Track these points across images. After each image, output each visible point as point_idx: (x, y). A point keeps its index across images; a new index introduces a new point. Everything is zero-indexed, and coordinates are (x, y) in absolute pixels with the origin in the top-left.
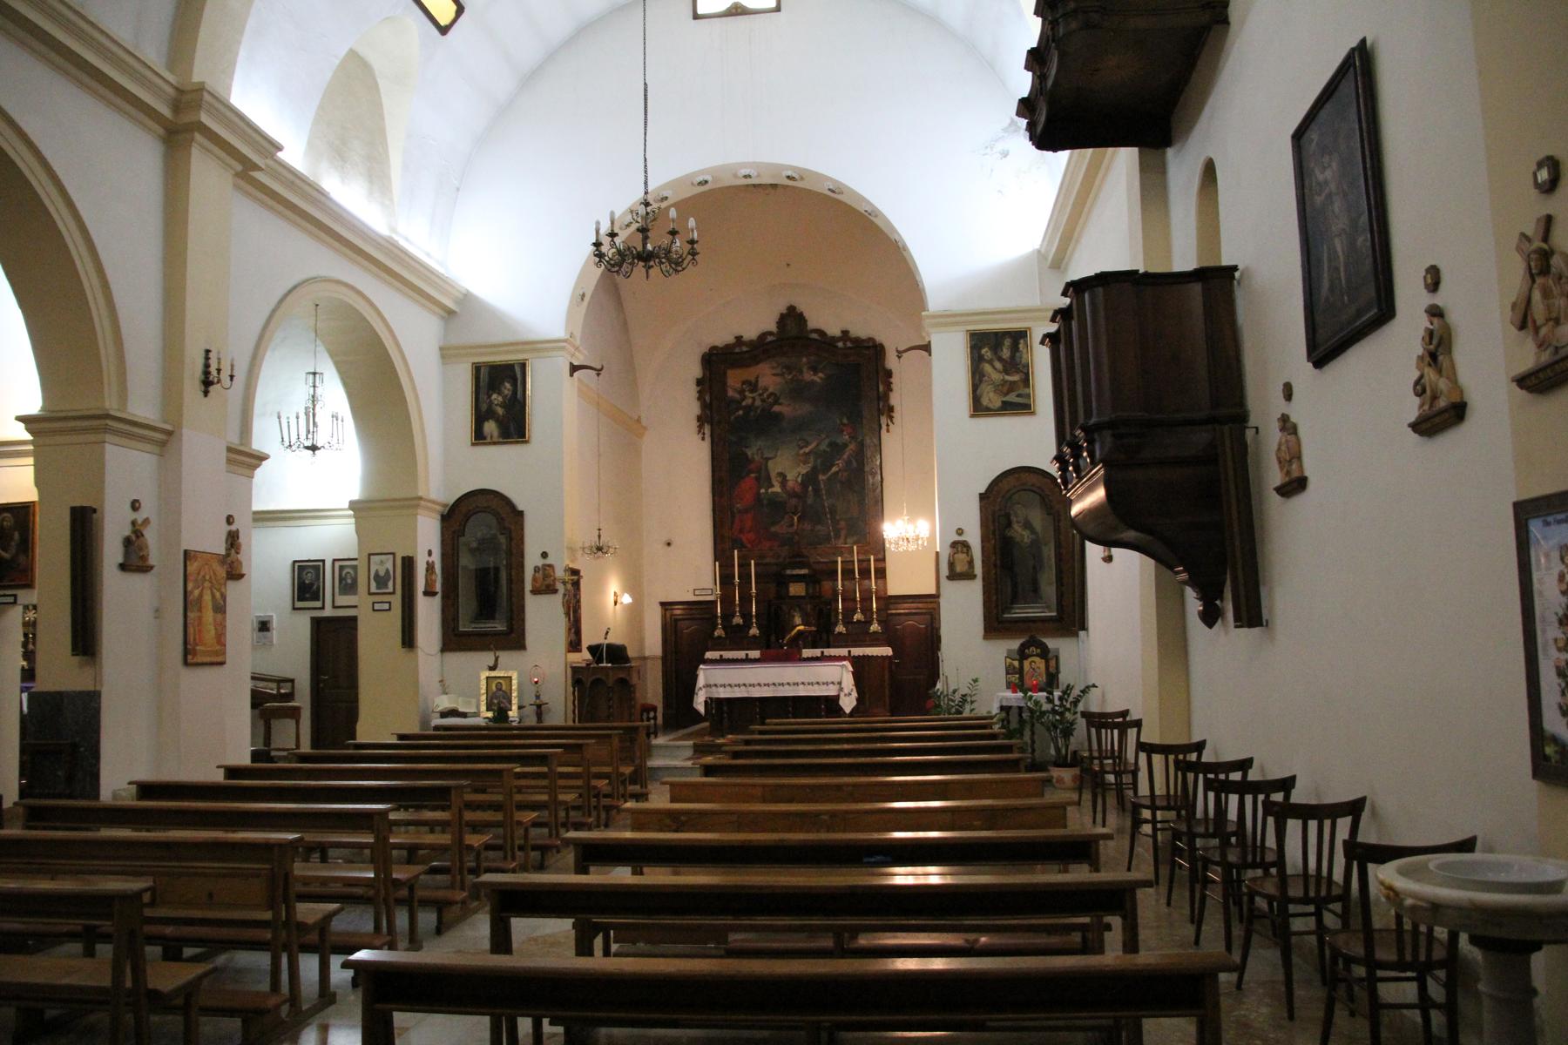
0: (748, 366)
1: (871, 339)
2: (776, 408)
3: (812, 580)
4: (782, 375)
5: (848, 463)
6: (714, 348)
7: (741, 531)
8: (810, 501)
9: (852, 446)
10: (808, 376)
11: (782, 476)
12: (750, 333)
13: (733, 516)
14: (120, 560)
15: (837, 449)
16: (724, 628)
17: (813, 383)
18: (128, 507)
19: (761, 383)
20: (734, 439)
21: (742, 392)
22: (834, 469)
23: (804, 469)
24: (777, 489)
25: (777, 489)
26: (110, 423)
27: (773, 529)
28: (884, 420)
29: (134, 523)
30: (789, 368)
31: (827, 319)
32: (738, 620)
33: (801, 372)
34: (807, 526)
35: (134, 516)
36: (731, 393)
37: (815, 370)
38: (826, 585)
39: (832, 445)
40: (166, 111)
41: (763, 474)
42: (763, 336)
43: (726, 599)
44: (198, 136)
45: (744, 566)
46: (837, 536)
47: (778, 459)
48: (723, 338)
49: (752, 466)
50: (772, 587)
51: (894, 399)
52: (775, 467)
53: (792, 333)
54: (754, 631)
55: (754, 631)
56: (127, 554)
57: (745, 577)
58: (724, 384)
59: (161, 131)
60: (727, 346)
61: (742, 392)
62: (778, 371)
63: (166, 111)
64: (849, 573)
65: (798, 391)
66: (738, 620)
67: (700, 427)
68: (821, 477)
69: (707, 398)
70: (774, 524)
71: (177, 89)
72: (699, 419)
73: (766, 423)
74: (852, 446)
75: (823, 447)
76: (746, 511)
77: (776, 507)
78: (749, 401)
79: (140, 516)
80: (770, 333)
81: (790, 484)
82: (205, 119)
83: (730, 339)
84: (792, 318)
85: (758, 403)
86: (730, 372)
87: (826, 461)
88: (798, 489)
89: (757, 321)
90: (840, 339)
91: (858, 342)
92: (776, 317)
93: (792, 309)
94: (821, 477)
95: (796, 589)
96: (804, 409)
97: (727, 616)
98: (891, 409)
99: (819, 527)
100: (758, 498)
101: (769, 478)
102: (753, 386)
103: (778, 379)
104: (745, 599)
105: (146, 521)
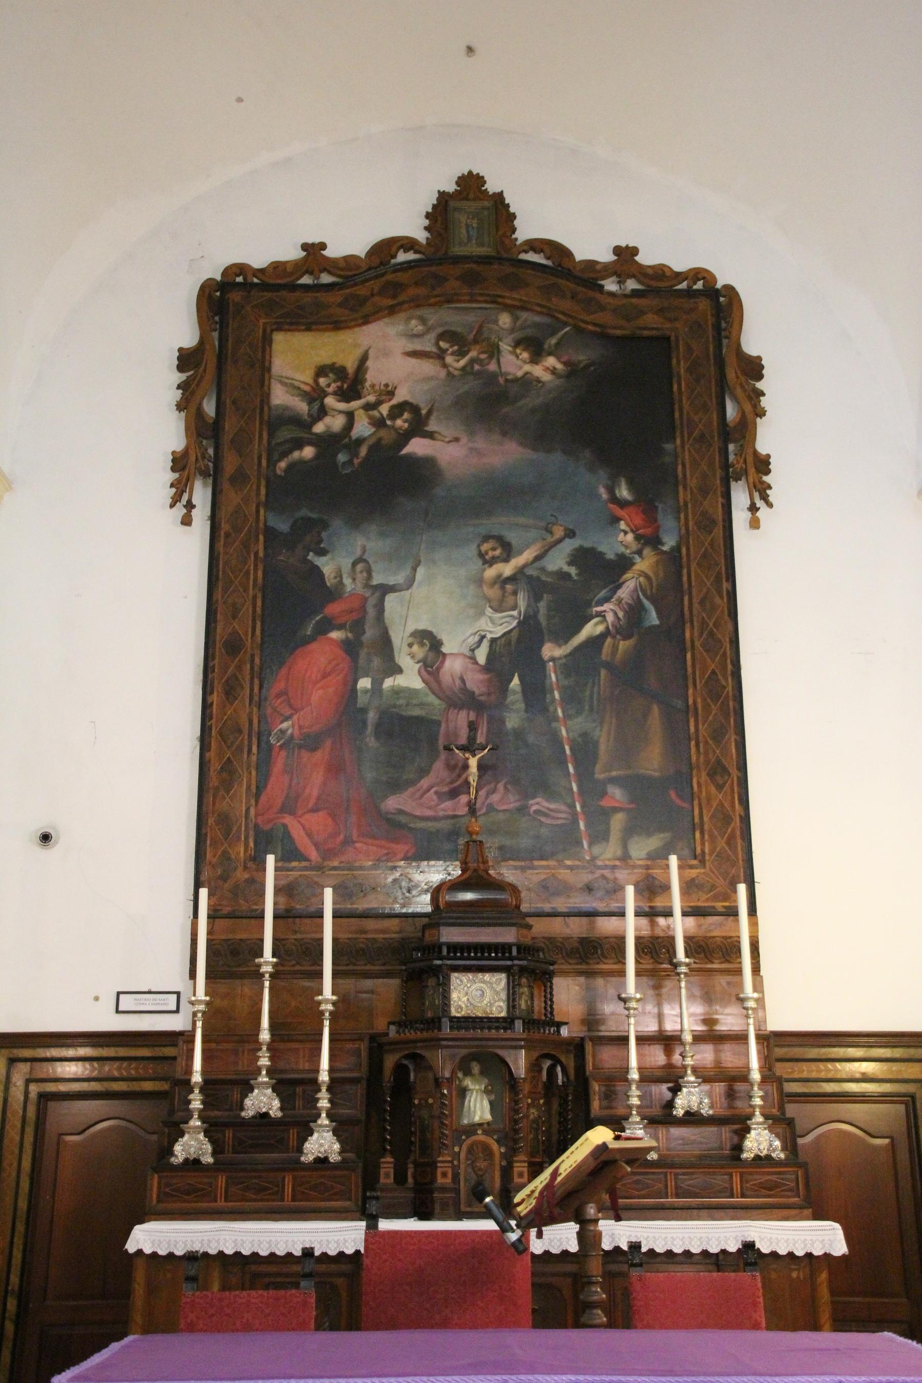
0: (337, 325)
1: (698, 274)
2: (417, 447)
3: (530, 966)
4: (440, 356)
5: (635, 611)
6: (241, 269)
7: (289, 807)
8: (512, 721)
9: (644, 564)
10: (514, 363)
11: (430, 642)
12: (349, 241)
13: (267, 752)
15: (603, 571)
16: (212, 1130)
17: (527, 382)
19: (376, 375)
20: (283, 525)
21: (315, 396)
22: (591, 629)
23: (499, 625)
24: (410, 679)
25: (410, 679)
27: (392, 803)
28: (740, 497)
30: (458, 340)
31: (570, 212)
32: (263, 1100)
33: (494, 352)
34: (502, 798)
36: (280, 397)
37: (537, 353)
38: (568, 995)
39: (586, 558)
41: (370, 633)
42: (385, 249)
43: (227, 1029)
45: (296, 916)
46: (600, 836)
47: (418, 591)
48: (268, 245)
49: (333, 609)
50: (385, 991)
51: (767, 440)
52: (404, 616)
53: (469, 250)
54: (322, 1143)
55: (322, 1143)
57: (299, 956)
58: (266, 369)
60: (277, 267)
61: (315, 396)
62: (427, 345)
64: (655, 950)
65: (488, 404)
66: (263, 1100)
67: (181, 489)
68: (550, 651)
69: (210, 408)
70: (395, 786)
72: (179, 462)
73: (382, 483)
74: (644, 564)
75: (558, 561)
76: (311, 742)
77: (408, 735)
78: (336, 423)
80: (408, 244)
81: (453, 667)
83: (291, 253)
84: (471, 208)
85: (362, 428)
86: (279, 339)
87: (560, 602)
88: (476, 682)
89: (370, 209)
90: (607, 270)
91: (659, 281)
92: (428, 201)
93: (471, 184)
94: (550, 651)
95: (476, 994)
96: (503, 454)
97: (225, 1088)
98: (763, 464)
99: (538, 803)
100: (349, 707)
101: (385, 644)
102: (351, 384)
103: (428, 368)
104: (295, 1030)
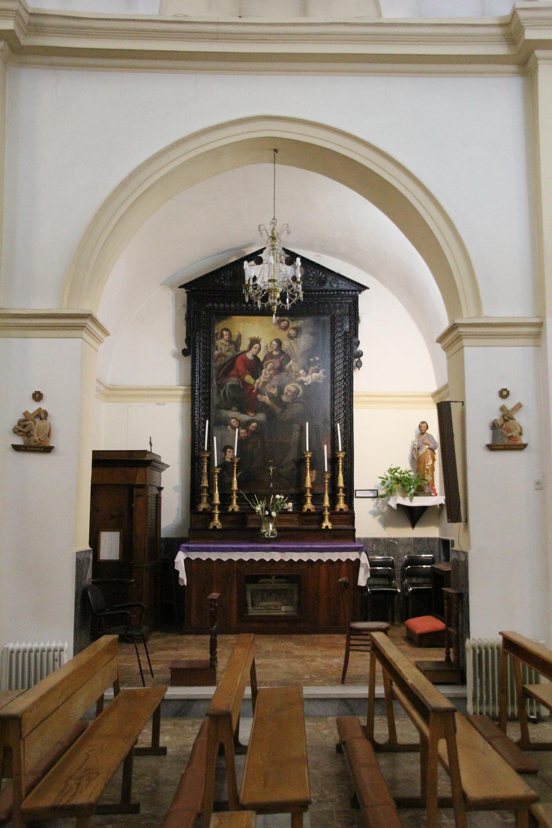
14: (488, 441)
18: (496, 395)
26: (461, 329)
29: (503, 409)
35: (502, 402)
40: (501, 50)
44: (538, 53)
56: (494, 436)
59: (512, 68)
63: (501, 50)
71: (501, 25)
79: (509, 404)
82: (530, 35)
105: (519, 406)
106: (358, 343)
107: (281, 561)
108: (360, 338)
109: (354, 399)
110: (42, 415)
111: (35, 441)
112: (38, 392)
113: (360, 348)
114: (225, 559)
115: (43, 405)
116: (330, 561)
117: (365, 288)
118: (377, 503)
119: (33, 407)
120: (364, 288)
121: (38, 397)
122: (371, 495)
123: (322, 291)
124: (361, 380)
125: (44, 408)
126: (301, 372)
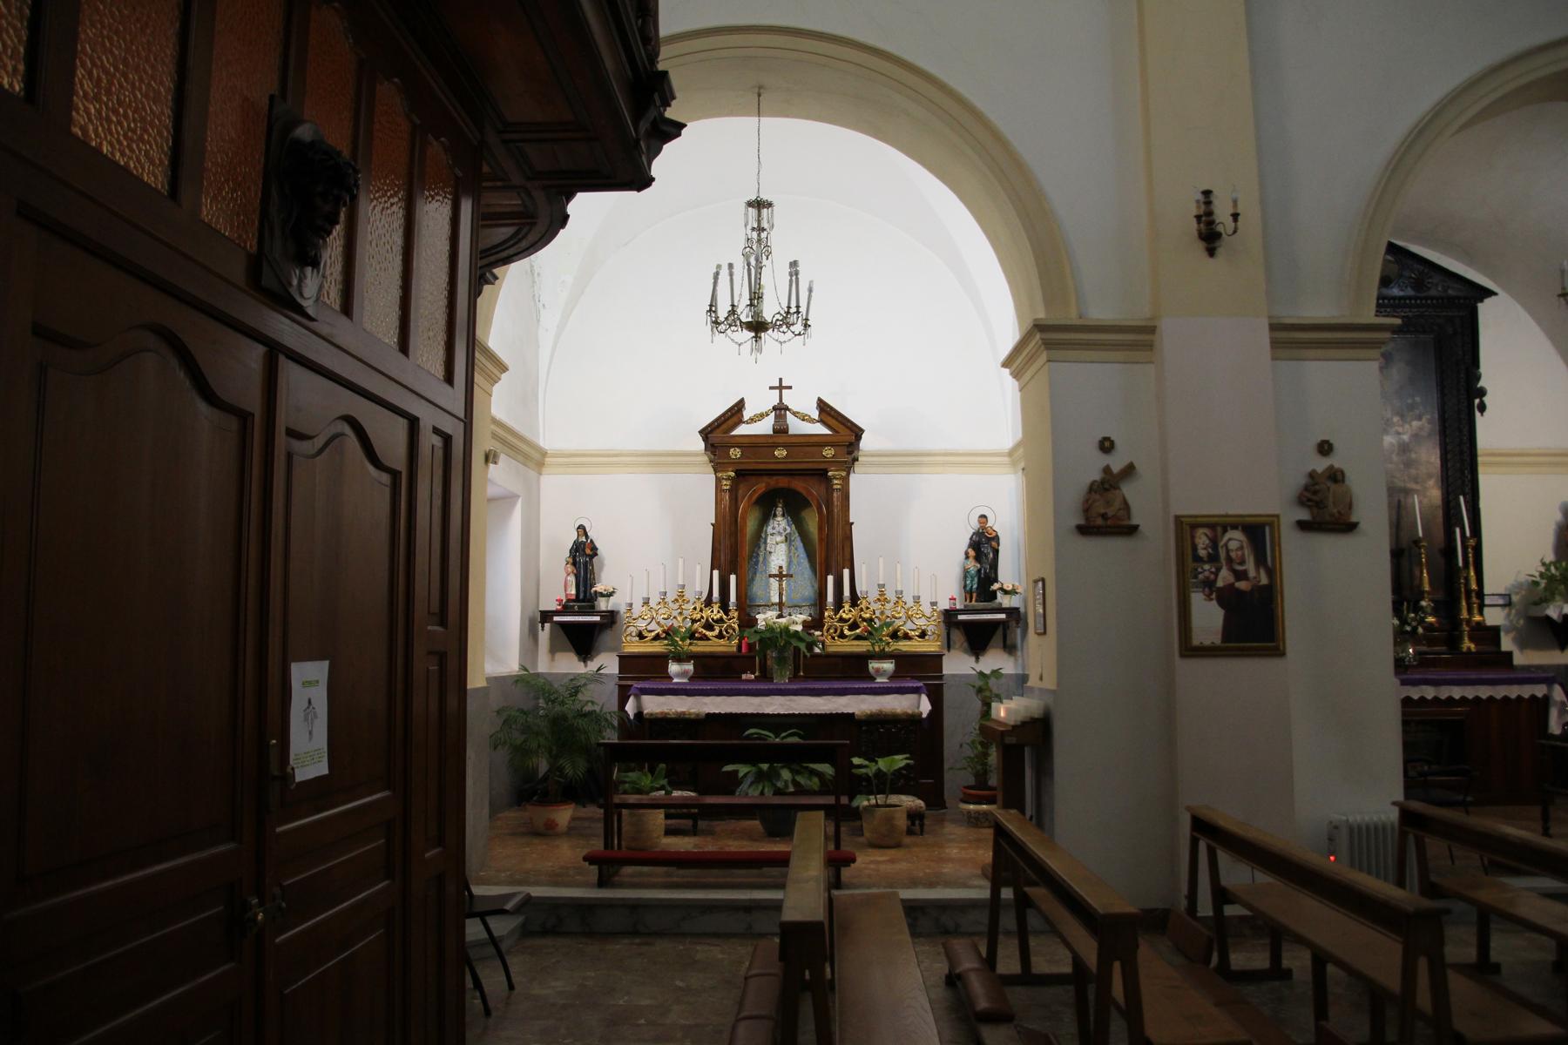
106: (1478, 378)
107: (1491, 698)
108: (1483, 369)
109: (1480, 459)
110: (1336, 476)
111: (1332, 515)
112: (1327, 442)
113: (1481, 384)
114: (1498, 697)
115: (1335, 461)
116: (1506, 698)
117: (1489, 293)
118: (1508, 615)
119: (1321, 464)
120: (1489, 293)
121: (1325, 448)
122: (1501, 602)
123: (1426, 298)
124: (1489, 432)
125: (1337, 465)
126: (1396, 419)
